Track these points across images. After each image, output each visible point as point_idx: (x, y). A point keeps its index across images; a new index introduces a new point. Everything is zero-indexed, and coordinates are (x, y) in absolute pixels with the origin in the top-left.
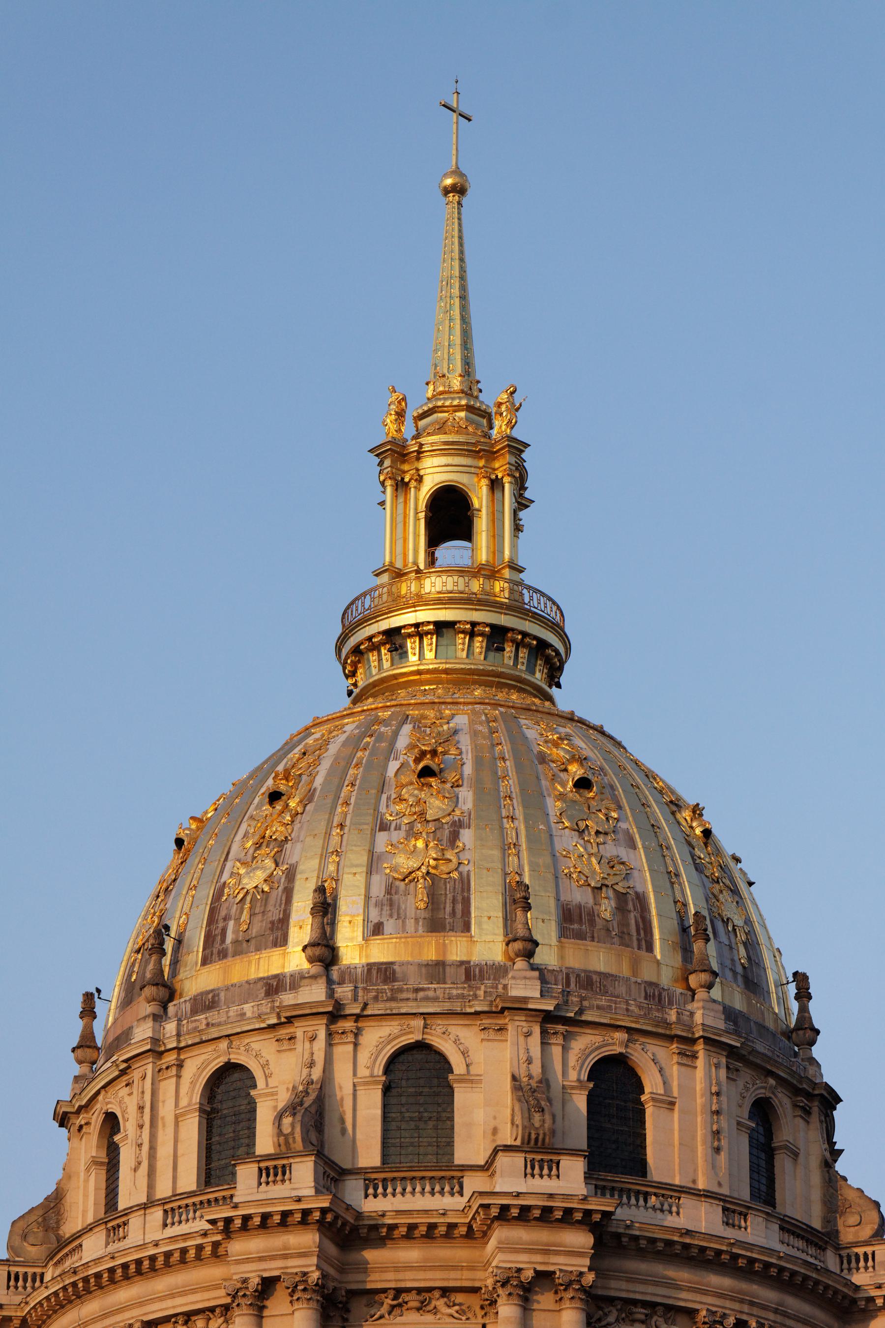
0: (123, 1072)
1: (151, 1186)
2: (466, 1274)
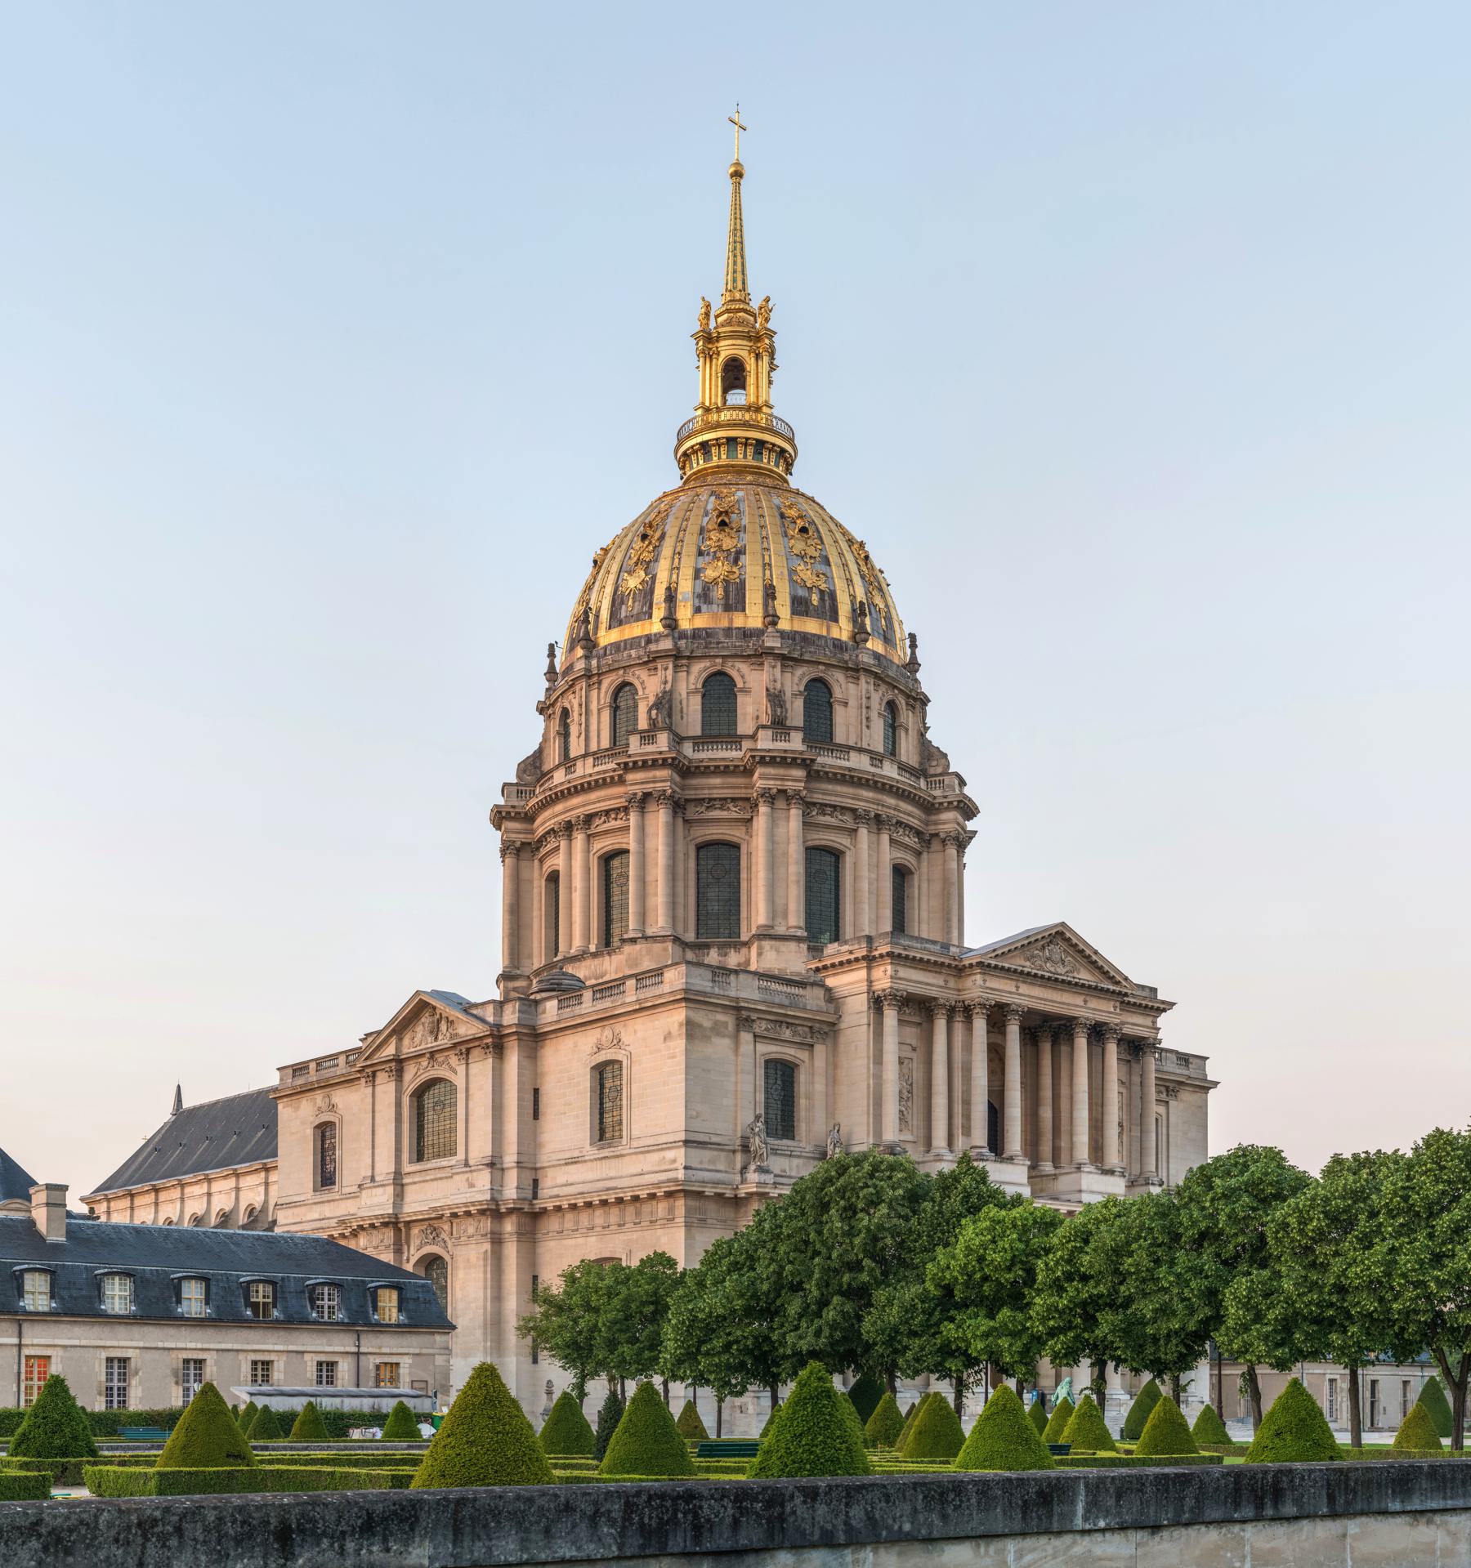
0: (571, 686)
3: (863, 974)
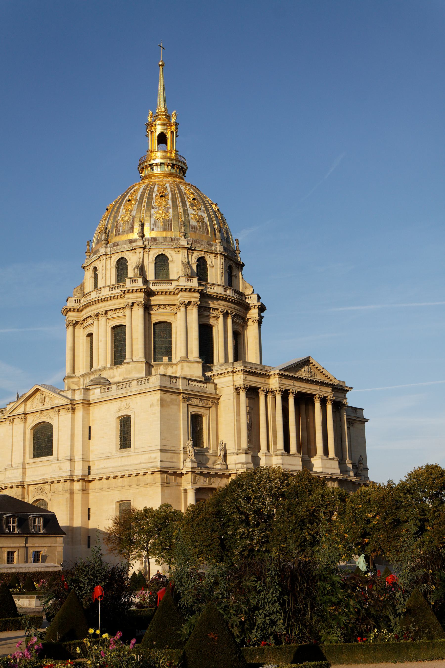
1: (105, 283)
2: (173, 302)
3: (231, 378)
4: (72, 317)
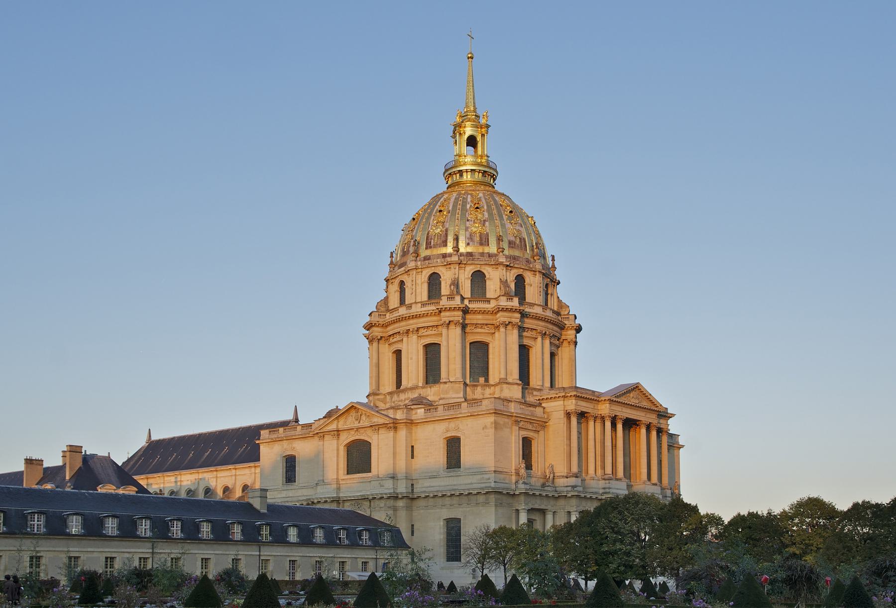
4: (377, 332)
